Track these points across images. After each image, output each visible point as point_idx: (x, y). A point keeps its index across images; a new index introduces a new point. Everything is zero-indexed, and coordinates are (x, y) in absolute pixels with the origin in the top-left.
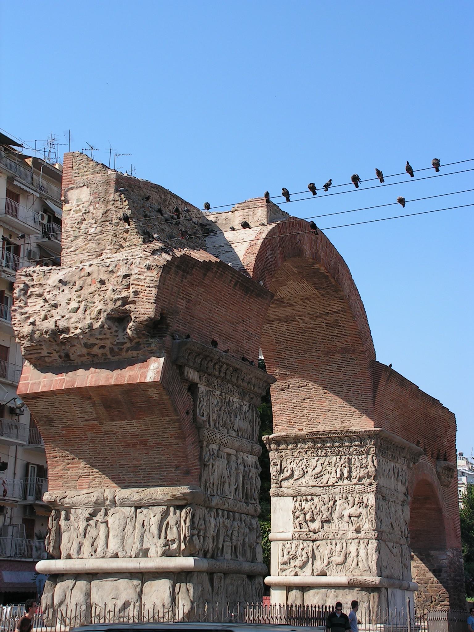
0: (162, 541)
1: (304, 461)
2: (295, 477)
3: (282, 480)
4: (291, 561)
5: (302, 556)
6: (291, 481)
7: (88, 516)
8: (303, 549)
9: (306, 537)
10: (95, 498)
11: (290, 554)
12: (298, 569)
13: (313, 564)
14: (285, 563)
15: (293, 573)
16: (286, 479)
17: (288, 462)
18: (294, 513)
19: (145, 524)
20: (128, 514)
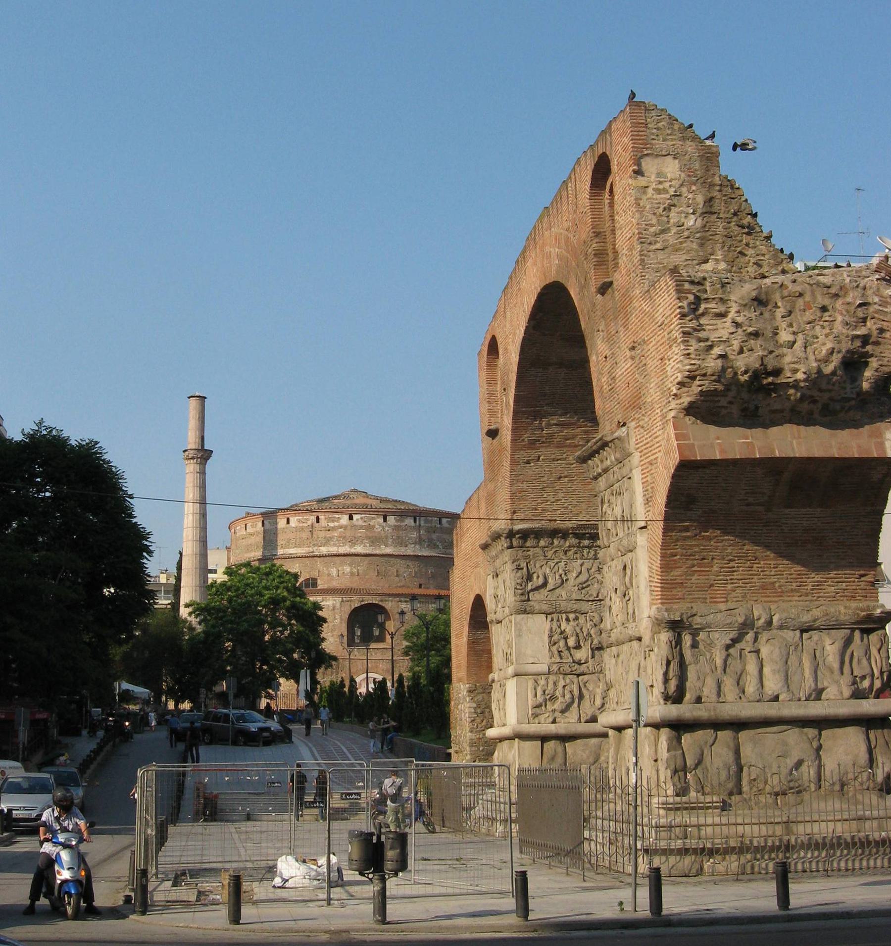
0: (846, 679)
1: (562, 564)
2: (550, 586)
3: (532, 590)
4: (548, 703)
5: (564, 697)
6: (544, 592)
7: (730, 642)
8: (564, 687)
9: (570, 670)
10: (744, 618)
11: (546, 693)
12: (557, 714)
13: (579, 706)
14: (539, 706)
15: (551, 720)
16: (537, 589)
17: (538, 565)
18: (550, 636)
19: (817, 655)
20: (791, 640)
